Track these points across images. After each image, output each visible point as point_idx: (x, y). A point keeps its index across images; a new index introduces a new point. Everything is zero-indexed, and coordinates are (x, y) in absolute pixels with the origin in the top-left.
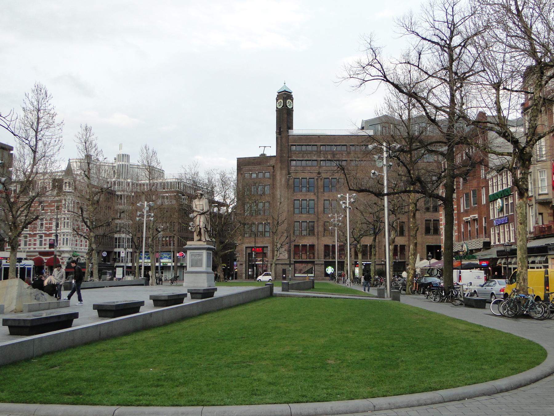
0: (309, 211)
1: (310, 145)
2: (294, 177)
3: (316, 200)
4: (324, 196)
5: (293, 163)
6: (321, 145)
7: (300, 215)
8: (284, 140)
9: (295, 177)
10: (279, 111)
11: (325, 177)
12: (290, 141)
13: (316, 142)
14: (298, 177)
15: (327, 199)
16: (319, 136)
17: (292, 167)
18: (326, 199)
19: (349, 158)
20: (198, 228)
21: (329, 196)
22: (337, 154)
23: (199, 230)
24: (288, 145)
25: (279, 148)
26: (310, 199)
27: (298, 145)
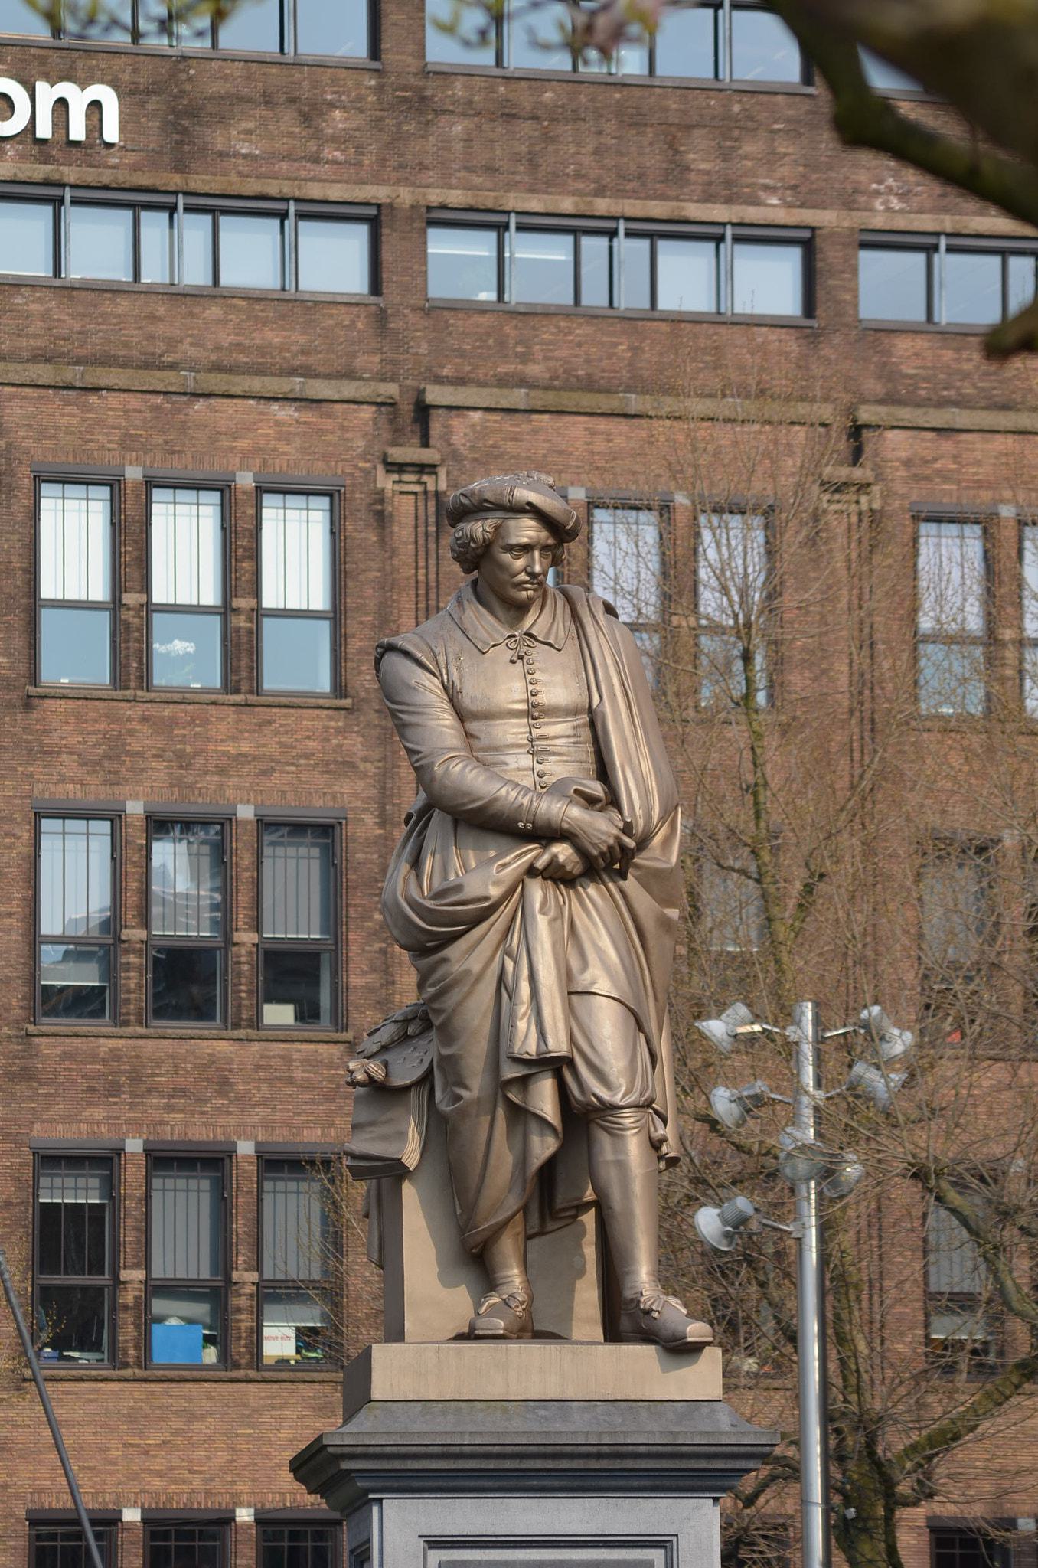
4: (43, 751)
18: (72, 792)
19: (410, 171)
20: (544, 1098)
21: (116, 751)
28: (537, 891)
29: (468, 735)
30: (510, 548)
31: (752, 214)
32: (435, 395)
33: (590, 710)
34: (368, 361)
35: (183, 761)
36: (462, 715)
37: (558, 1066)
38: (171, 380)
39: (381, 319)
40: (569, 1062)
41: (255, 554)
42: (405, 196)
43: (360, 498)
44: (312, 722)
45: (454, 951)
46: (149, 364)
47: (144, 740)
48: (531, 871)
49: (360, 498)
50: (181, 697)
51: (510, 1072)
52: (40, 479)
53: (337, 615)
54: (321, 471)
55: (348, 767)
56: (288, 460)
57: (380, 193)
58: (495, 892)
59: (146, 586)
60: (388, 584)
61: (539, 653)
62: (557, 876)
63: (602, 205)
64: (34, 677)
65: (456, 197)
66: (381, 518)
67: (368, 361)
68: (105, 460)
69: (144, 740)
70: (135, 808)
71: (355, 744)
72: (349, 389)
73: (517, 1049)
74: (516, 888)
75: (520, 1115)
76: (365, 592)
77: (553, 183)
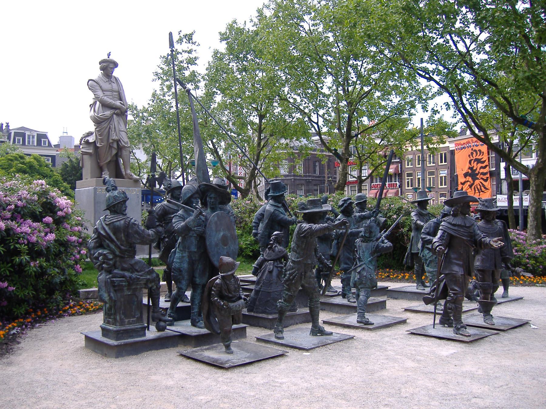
20: (115, 146)
23: (114, 152)
28: (115, 116)
29: (104, 93)
30: (110, 68)
33: (119, 92)
36: (103, 91)
37: (118, 141)
40: (120, 140)
45: (103, 123)
48: (114, 113)
51: (111, 141)
58: (110, 116)
61: (112, 83)
62: (117, 115)
73: (113, 138)
74: (112, 117)
75: (111, 147)
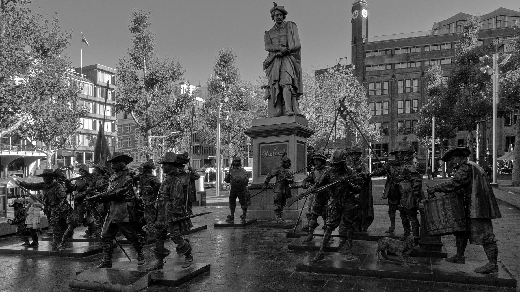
0: (383, 112)
1: (385, 50)
2: (369, 81)
3: (390, 102)
4: (398, 97)
5: (368, 69)
6: (395, 49)
7: (375, 117)
8: (359, 48)
9: (371, 82)
10: (353, 21)
11: (399, 79)
12: (365, 49)
13: (390, 47)
14: (372, 81)
15: (402, 99)
16: (393, 41)
17: (368, 73)
22: (411, 56)
24: (364, 53)
25: (355, 56)
26: (384, 101)
27: (373, 52)
31: (447, 57)
32: (425, 72)
34: (420, 70)
35: (408, 97)
38: (407, 74)
39: (421, 68)
41: (412, 83)
42: (423, 60)
43: (419, 79)
44: (416, 93)
46: (406, 73)
47: (405, 96)
49: (419, 79)
50: (407, 93)
52: (398, 80)
53: (418, 87)
54: (417, 78)
55: (418, 96)
56: (415, 77)
57: (421, 60)
59: (405, 86)
60: (422, 84)
63: (437, 58)
64: (398, 93)
65: (426, 59)
66: (421, 80)
67: (420, 70)
68: (403, 78)
69: (405, 96)
70: (404, 100)
71: (419, 95)
72: (419, 72)
76: (420, 85)
77: (433, 58)
